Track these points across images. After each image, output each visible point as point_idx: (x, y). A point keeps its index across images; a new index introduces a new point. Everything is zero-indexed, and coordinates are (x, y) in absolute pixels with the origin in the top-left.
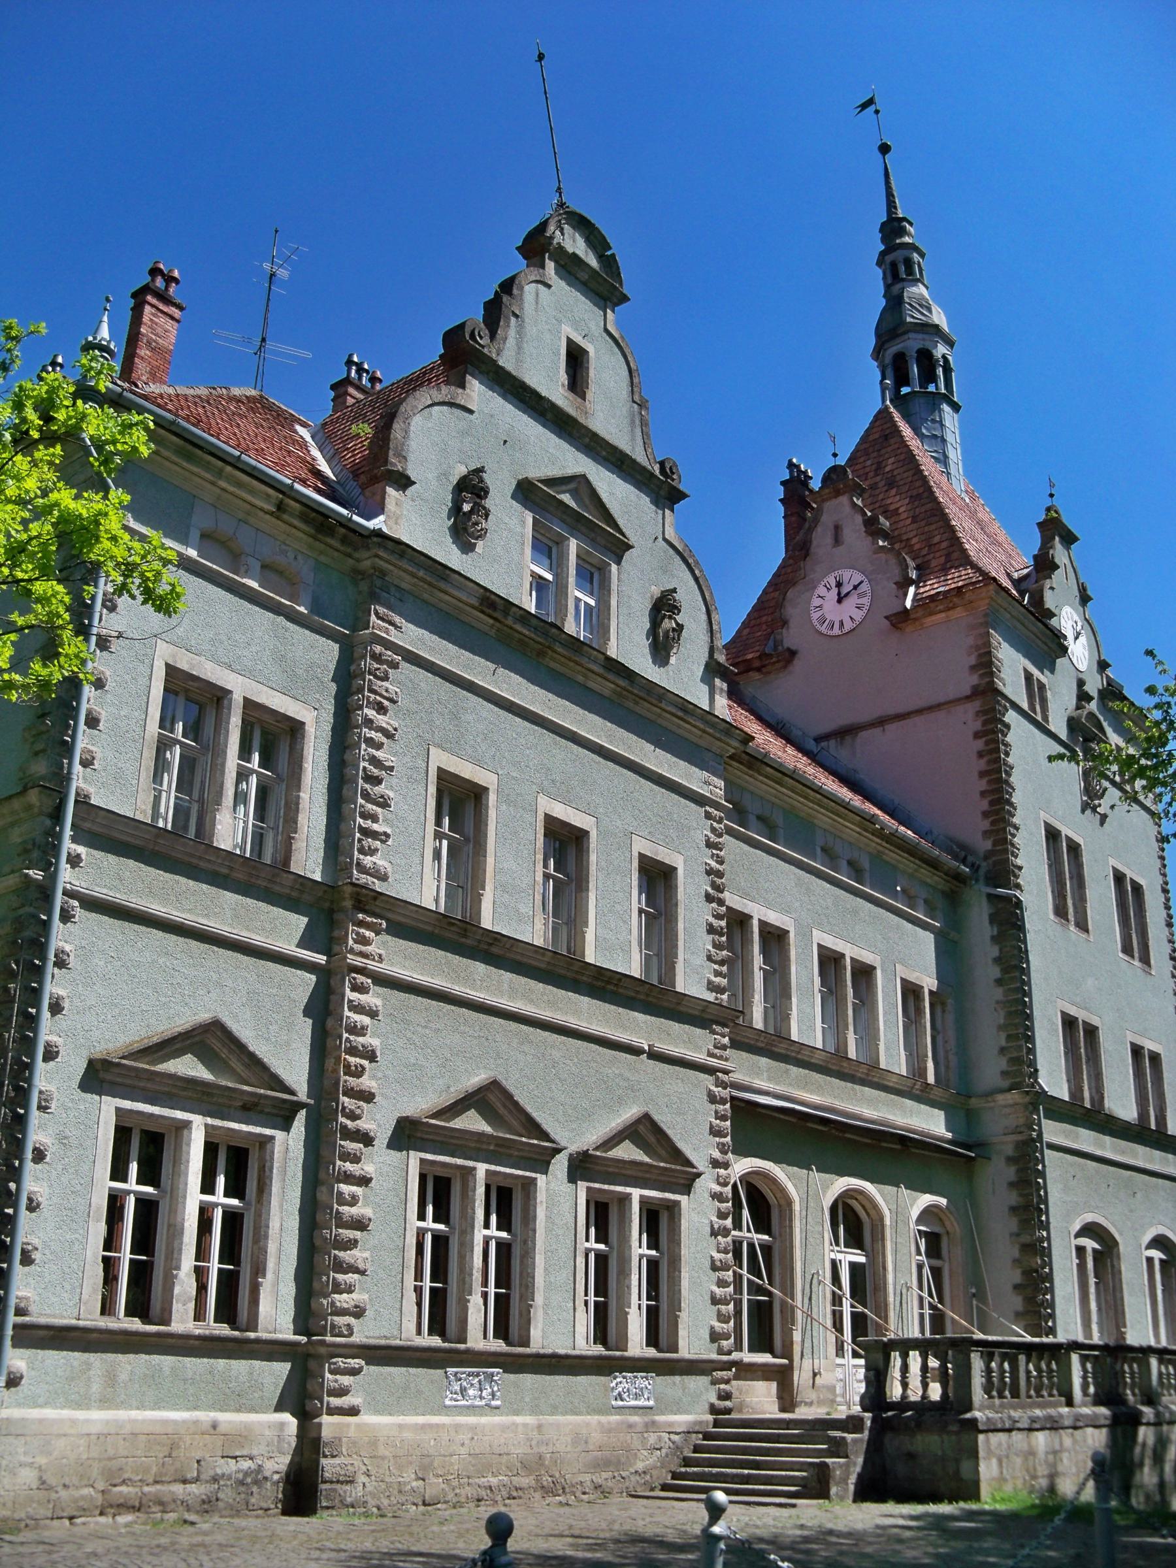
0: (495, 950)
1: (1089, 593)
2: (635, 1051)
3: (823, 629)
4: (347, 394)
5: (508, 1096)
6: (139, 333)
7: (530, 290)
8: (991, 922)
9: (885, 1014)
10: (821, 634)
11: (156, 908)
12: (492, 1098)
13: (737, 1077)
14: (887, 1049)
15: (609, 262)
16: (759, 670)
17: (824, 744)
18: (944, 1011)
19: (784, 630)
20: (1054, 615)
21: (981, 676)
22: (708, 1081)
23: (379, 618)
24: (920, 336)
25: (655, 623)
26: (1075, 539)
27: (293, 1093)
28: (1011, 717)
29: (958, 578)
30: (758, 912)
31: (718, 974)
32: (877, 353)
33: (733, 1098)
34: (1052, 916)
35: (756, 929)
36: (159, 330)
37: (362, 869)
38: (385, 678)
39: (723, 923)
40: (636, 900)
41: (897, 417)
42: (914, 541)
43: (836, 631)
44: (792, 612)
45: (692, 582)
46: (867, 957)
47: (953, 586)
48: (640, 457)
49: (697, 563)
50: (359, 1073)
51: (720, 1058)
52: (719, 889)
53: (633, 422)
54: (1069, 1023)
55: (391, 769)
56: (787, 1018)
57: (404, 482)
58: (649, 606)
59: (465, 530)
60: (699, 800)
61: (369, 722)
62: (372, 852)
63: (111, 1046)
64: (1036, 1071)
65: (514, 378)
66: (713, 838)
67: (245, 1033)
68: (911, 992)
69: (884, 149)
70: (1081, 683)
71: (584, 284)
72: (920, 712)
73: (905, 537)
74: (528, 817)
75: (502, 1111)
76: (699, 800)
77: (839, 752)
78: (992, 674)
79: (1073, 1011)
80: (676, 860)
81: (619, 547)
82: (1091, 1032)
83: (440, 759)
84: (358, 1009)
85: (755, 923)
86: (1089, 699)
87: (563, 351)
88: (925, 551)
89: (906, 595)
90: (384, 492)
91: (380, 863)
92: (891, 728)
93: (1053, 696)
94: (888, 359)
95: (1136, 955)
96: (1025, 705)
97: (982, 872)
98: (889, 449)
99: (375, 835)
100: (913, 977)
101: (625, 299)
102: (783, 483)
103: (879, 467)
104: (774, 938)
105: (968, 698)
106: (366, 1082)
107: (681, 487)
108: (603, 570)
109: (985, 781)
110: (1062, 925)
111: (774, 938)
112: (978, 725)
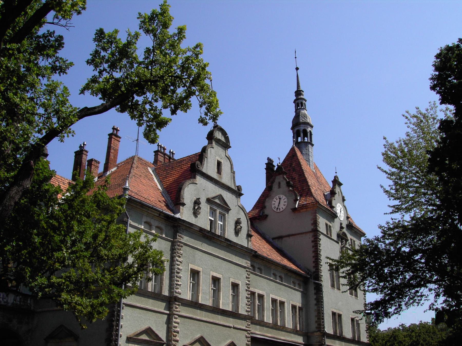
0: (202, 307)
1: (345, 199)
2: (230, 327)
3: (275, 210)
4: (158, 154)
5: (204, 339)
6: (111, 146)
7: (209, 150)
8: (315, 289)
9: (287, 313)
11: (138, 305)
12: (201, 339)
13: (253, 331)
14: (288, 322)
15: (227, 138)
16: (258, 219)
17: (274, 240)
18: (302, 311)
19: (265, 209)
20: (334, 207)
21: (314, 226)
22: (246, 333)
23: (179, 236)
24: (304, 126)
25: (236, 227)
26: (342, 184)
27: (163, 341)
28: (321, 237)
29: (309, 200)
30: (257, 291)
31: (248, 308)
32: (292, 128)
33: (251, 337)
34: (330, 287)
35: (257, 296)
36: (115, 145)
37: (176, 293)
38: (180, 250)
39: (249, 296)
40: (231, 292)
41: (296, 149)
42: (299, 188)
43: (278, 211)
44: (267, 204)
45: (244, 215)
46: (283, 300)
48: (233, 187)
49: (245, 210)
50: (175, 336)
51: (248, 328)
52: (249, 288)
53: (231, 178)
54: (334, 314)
55: (181, 270)
56: (263, 316)
57: (183, 204)
58: (234, 222)
59: (196, 213)
60: (244, 267)
61: (177, 260)
62: (178, 289)
63: (130, 334)
64: (324, 327)
65: (206, 174)
66: (248, 276)
67: (154, 329)
68: (294, 307)
69: (297, 69)
70: (341, 224)
71: (221, 145)
73: (297, 186)
74: (208, 277)
75: (203, 342)
76: (244, 267)
77: (278, 243)
78: (317, 226)
79: (335, 311)
80: (239, 282)
81: (227, 209)
82: (340, 316)
83: (191, 266)
84: (176, 323)
85: (257, 294)
86: (344, 228)
87: (216, 164)
89: (296, 203)
90: (180, 208)
91: (180, 291)
92: (291, 237)
93: (333, 229)
94: (295, 132)
95: (354, 294)
96: (325, 233)
97: (312, 277)
98: (294, 160)
99: (178, 285)
100: (294, 304)
101: (230, 147)
102: (266, 164)
103: (291, 164)
104: (261, 297)
105: (310, 232)
106: (177, 338)
107: (242, 192)
108: (224, 215)
109: (314, 253)
110: (333, 289)
112: (313, 239)
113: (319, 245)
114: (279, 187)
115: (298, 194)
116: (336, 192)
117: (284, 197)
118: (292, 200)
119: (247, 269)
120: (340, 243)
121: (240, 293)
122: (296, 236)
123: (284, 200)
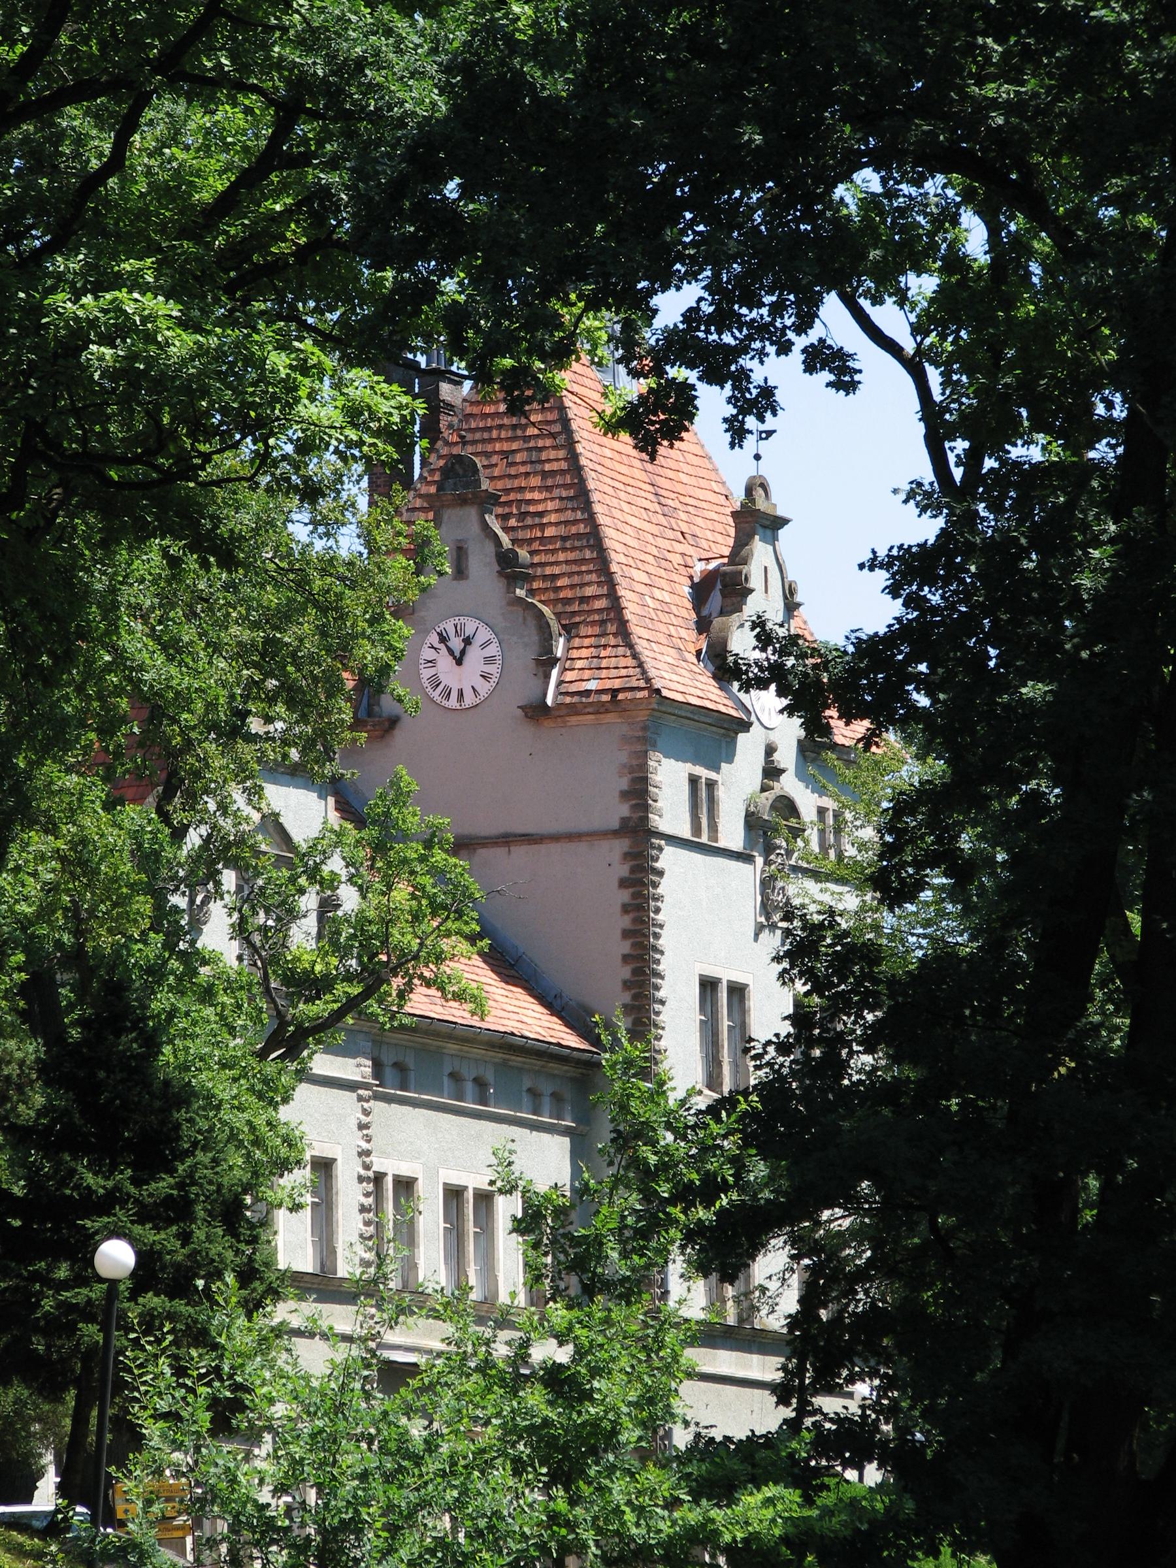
3: (435, 695)
10: (432, 700)
21: (634, 808)
39: (371, 1200)
43: (453, 703)
47: (608, 684)
70: (770, 750)
72: (555, 838)
78: (646, 808)
88: (575, 607)
89: (547, 676)
92: (520, 853)
96: (685, 832)
104: (405, 1185)
111: (405, 1185)
112: (624, 870)
113: (652, 903)
114: (460, 572)
115: (555, 626)
116: (756, 582)
117: (484, 634)
118: (526, 655)
119: (360, 1092)
120: (760, 861)
121: (341, 1194)
122: (543, 848)
123: (484, 646)
